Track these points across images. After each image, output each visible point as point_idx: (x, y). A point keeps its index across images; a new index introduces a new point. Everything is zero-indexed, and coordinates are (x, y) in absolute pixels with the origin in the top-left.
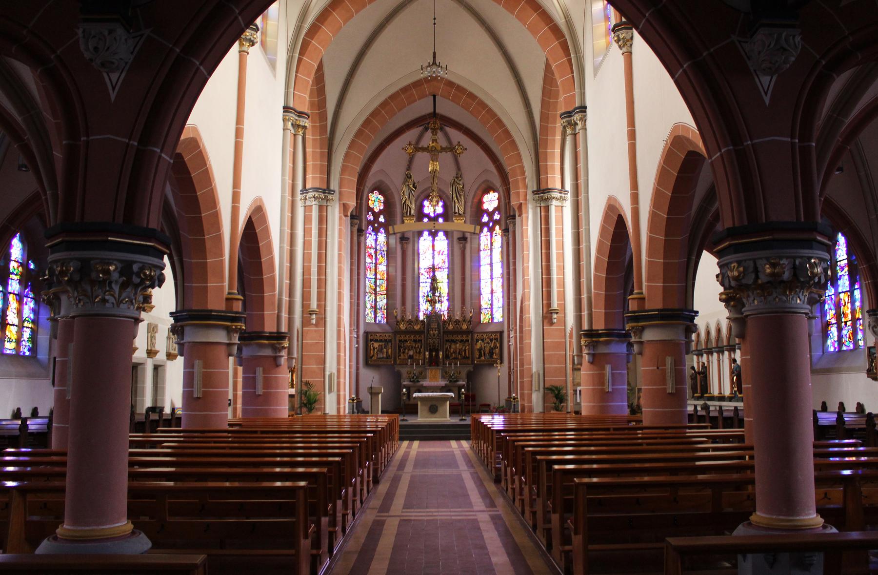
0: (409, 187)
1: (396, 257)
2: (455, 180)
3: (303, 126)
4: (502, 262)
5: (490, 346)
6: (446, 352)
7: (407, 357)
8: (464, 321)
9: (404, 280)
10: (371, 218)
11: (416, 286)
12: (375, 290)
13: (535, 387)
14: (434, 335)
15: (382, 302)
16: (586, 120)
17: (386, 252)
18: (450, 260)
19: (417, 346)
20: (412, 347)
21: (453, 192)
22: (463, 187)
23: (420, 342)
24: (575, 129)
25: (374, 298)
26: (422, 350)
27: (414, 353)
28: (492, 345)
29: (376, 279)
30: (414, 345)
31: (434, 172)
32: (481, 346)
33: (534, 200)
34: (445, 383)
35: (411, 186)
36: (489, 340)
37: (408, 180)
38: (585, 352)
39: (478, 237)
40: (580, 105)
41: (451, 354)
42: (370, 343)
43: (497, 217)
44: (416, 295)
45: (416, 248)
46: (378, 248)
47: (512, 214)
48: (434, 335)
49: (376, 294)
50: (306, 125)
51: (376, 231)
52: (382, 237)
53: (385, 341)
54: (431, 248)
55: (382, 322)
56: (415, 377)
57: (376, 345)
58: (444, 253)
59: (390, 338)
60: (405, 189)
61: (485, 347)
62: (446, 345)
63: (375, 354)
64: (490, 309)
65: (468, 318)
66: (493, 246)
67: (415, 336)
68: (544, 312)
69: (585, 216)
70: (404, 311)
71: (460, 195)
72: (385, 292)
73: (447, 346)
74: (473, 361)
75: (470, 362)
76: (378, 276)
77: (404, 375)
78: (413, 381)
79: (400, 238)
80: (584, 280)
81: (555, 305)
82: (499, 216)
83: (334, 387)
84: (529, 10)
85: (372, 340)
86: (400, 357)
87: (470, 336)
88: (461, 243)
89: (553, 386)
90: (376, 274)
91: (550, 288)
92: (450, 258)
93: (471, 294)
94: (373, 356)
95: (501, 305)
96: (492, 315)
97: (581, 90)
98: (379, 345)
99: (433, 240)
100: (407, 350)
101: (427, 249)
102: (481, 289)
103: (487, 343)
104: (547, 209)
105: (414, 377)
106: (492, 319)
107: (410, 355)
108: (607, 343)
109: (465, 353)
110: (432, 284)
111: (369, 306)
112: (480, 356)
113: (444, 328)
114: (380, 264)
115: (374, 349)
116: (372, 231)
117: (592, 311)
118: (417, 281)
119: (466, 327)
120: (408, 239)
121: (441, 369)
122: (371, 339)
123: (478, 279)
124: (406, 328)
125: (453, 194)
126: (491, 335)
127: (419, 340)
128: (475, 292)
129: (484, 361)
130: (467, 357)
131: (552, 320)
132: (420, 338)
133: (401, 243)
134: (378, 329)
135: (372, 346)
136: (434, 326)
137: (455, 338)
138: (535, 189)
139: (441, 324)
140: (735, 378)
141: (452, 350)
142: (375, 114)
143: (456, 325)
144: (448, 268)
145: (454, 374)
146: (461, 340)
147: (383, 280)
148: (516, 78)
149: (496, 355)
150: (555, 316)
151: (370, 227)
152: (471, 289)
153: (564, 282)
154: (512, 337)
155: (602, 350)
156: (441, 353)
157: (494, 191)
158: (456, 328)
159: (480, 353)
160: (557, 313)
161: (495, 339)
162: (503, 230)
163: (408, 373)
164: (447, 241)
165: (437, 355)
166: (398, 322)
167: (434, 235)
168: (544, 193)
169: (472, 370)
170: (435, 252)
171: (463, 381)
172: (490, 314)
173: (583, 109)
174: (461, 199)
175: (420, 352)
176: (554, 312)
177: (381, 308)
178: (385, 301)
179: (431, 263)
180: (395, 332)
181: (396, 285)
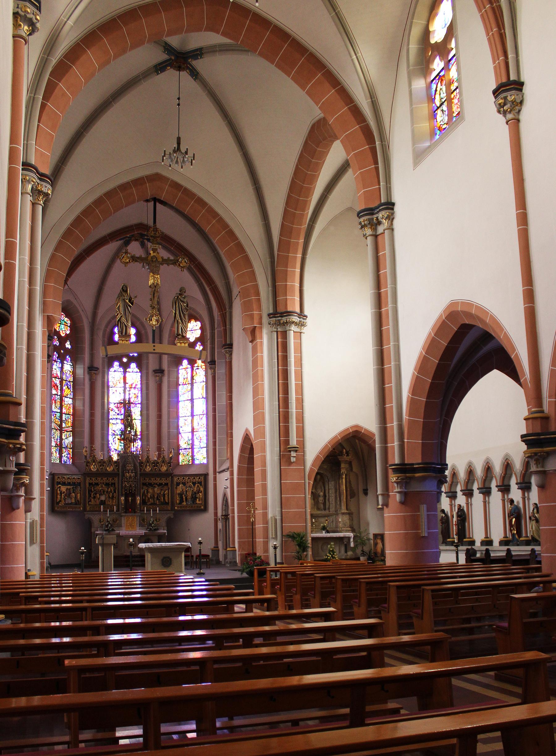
0: (125, 302)
1: (83, 390)
2: (178, 297)
3: (45, 193)
4: (206, 398)
6: (143, 497)
8: (163, 462)
9: (92, 415)
10: (57, 343)
11: (106, 422)
12: (60, 426)
13: (272, 535)
14: (130, 477)
15: (68, 440)
16: (393, 219)
17: (72, 383)
18: (144, 395)
21: (176, 311)
22: (187, 306)
23: (113, 486)
24: (375, 230)
25: (59, 435)
27: (106, 499)
28: (195, 489)
29: (61, 413)
31: (155, 287)
33: (269, 324)
34: (145, 531)
35: (127, 301)
36: (191, 483)
37: (124, 293)
38: (396, 490)
39: (176, 370)
40: (386, 201)
41: (149, 499)
42: (56, 487)
43: (199, 347)
44: (106, 432)
45: (106, 380)
46: (64, 377)
47: (228, 342)
48: (130, 477)
50: (49, 192)
51: (62, 359)
52: (68, 367)
53: (74, 484)
54: (122, 381)
55: (68, 463)
57: (64, 489)
58: (137, 387)
60: (120, 304)
61: (186, 491)
62: (142, 489)
63: (63, 500)
64: (190, 450)
66: (194, 380)
67: (107, 479)
68: (282, 450)
69: (394, 330)
70: (92, 450)
71: (184, 315)
74: (173, 509)
75: (169, 508)
76: (64, 411)
77: (96, 523)
78: (107, 530)
79: (89, 368)
80: (392, 405)
81: (293, 442)
82: (201, 348)
83: (37, 537)
84: (327, 85)
85: (59, 483)
88: (156, 376)
89: (295, 533)
90: (61, 408)
91: (288, 423)
92: (144, 392)
93: (169, 432)
94: (60, 501)
95: (204, 444)
96: (193, 456)
97: (387, 184)
98: (67, 489)
99: (125, 372)
101: (118, 382)
102: (180, 428)
103: (189, 487)
104: (285, 335)
105: (108, 525)
106: (193, 460)
107: (102, 501)
108: (424, 479)
109: (164, 499)
111: (53, 444)
112: (181, 501)
113: (141, 469)
114: (66, 397)
115: (61, 494)
116: (58, 358)
117: (403, 442)
118: (107, 417)
120: (97, 369)
122: (57, 482)
123: (176, 415)
124: (98, 470)
125: (175, 314)
126: (194, 478)
127: (112, 483)
128: (173, 430)
130: (166, 502)
131: (290, 459)
133: (89, 373)
134: (64, 471)
135: (59, 490)
136: (130, 467)
137: (153, 481)
138: (271, 311)
139: (138, 465)
140: (514, 520)
141: (149, 494)
142: (87, 212)
143: (154, 466)
144: (141, 404)
145: (153, 521)
147: (69, 414)
148: (255, 185)
149: (199, 501)
150: (293, 454)
151: (55, 353)
152: (169, 427)
153: (303, 417)
154: (226, 480)
155: (416, 487)
156: (138, 498)
157: (196, 320)
160: (296, 451)
161: (198, 483)
162: (208, 363)
163: (100, 520)
164: (140, 374)
165: (134, 500)
166: (88, 462)
167: (125, 366)
168: (282, 317)
169: (172, 517)
170: (127, 385)
171: (164, 530)
172: (190, 454)
173: (390, 206)
174: (186, 319)
175: (113, 497)
176: (293, 450)
177: (67, 446)
178: (71, 439)
179: (122, 398)
180: (84, 474)
181: (84, 420)
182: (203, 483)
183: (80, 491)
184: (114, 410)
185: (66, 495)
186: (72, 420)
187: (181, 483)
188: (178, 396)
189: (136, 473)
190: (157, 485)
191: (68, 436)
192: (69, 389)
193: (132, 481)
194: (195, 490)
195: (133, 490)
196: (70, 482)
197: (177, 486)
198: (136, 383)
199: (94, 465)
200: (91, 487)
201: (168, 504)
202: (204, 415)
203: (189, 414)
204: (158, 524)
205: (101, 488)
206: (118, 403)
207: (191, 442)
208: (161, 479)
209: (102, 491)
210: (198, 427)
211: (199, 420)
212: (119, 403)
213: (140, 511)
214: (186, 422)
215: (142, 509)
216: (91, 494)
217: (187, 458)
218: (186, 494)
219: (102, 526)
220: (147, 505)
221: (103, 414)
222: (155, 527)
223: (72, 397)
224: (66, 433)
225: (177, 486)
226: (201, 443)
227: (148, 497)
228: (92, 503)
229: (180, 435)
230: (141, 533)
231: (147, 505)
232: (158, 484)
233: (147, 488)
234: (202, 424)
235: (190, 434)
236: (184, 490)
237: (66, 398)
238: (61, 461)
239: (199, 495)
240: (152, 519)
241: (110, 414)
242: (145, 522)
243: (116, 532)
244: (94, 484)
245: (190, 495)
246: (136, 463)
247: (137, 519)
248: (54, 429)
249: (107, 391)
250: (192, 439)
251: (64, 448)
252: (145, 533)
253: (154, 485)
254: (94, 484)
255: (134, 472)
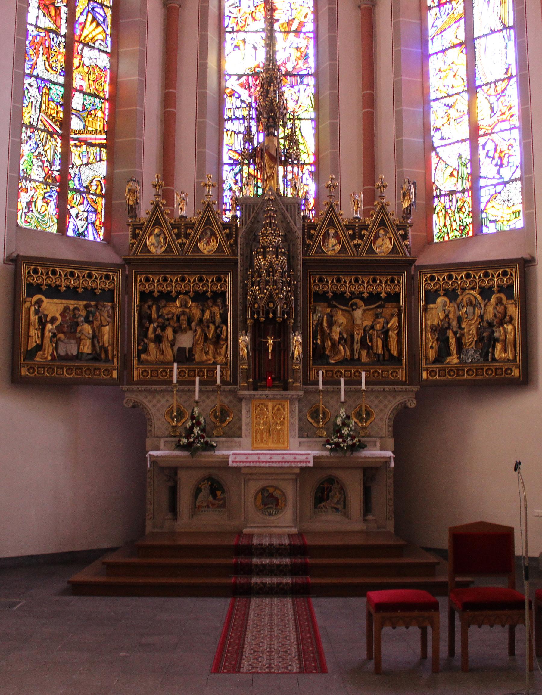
5: (481, 317)
6: (315, 338)
7: (169, 355)
8: (382, 224)
11: (211, 122)
12: (65, 124)
14: (271, 269)
17: (109, 12)
19: (207, 315)
20: (189, 322)
23: (219, 301)
25: (59, 150)
26: (227, 330)
27: (195, 343)
28: (490, 310)
30: (197, 313)
32: (447, 316)
34: (317, 453)
41: (334, 345)
44: (210, 153)
48: (271, 269)
49: (65, 138)
55: (91, 238)
56: (196, 430)
59: (107, 286)
61: (460, 320)
62: (314, 312)
63: (47, 341)
65: (395, 219)
67: (201, 280)
72: (102, 139)
73: (316, 317)
75: (402, 375)
76: (78, 81)
78: (188, 447)
85: (33, 289)
86: (143, 356)
87: (403, 279)
90: (68, 71)
93: (399, 145)
94: (39, 347)
98: (66, 309)
100: (169, 331)
103: (470, 303)
105: (192, 428)
106: (478, 224)
107: (182, 350)
110: (265, 93)
114: (86, 45)
115: (42, 322)
119: (391, 247)
121: (299, 400)
122: (30, 285)
124: (169, 250)
127: (214, 293)
129: (459, 370)
130: (391, 356)
132: (218, 288)
135: (37, 312)
139: (299, 233)
141: (336, 331)
143: (353, 237)
145: (348, 417)
146: (371, 293)
147: (95, 96)
156: (297, 339)
158: (351, 254)
159: (443, 341)
161: (501, 289)
163: (170, 413)
166: (138, 226)
169: (412, 404)
171: (382, 449)
172: (468, 208)
177: (87, 188)
178: (102, 169)
179: (261, 57)
180: (128, 262)
181: (142, 114)
182: (517, 291)
183: (112, 317)
184: (236, 95)
185: (60, 328)
186: (107, 113)
187: (441, 292)
188: (424, 42)
189: (291, 259)
190: (362, 299)
191: (92, 157)
192: (98, 25)
193: (275, 282)
194: (490, 314)
195: (279, 313)
196: (76, 288)
197: (427, 302)
198: (303, 20)
199: (158, 236)
200: (150, 307)
201: (398, 360)
202: (509, 79)
203: (461, 85)
204: (363, 428)
205: (180, 310)
206: (248, 75)
207: (469, 171)
208: (374, 281)
209: (182, 317)
210: (492, 121)
211: (493, 99)
212: (252, 75)
213: (305, 383)
214: (452, 112)
215: (312, 378)
216: (148, 329)
217: (458, 220)
218: (460, 327)
219: (174, 433)
220: (329, 364)
221: (201, 97)
222: (353, 438)
223: (109, 50)
224: (84, 148)
225: (427, 302)
226: (501, 170)
227: (331, 339)
228: (149, 358)
229: (433, 154)
230: (303, 458)
231: (329, 364)
232: (366, 295)
233: (328, 310)
234: (505, 109)
235: (467, 145)
236: (451, 316)
237: (86, 49)
238: (62, 228)
239: (505, 331)
240: (342, 411)
241: (228, 105)
242: (319, 422)
243: (217, 453)
244: (156, 294)
245: (473, 331)
246: (292, 224)
247: (292, 411)
248: (42, 130)
249: (216, 39)
250: (474, 161)
251: (77, 191)
252: (315, 457)
253: (351, 298)
254: (156, 294)
255: (284, 254)
